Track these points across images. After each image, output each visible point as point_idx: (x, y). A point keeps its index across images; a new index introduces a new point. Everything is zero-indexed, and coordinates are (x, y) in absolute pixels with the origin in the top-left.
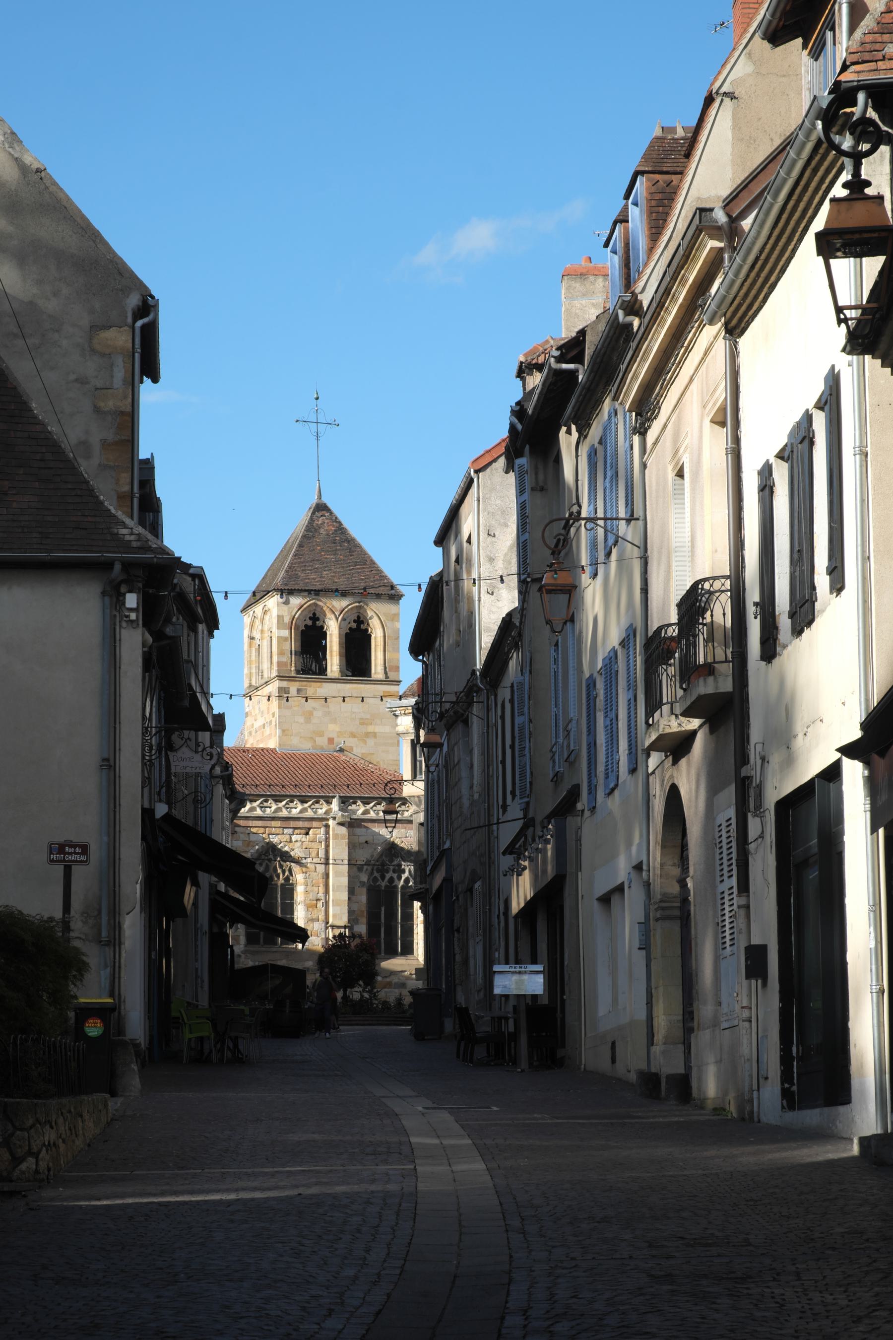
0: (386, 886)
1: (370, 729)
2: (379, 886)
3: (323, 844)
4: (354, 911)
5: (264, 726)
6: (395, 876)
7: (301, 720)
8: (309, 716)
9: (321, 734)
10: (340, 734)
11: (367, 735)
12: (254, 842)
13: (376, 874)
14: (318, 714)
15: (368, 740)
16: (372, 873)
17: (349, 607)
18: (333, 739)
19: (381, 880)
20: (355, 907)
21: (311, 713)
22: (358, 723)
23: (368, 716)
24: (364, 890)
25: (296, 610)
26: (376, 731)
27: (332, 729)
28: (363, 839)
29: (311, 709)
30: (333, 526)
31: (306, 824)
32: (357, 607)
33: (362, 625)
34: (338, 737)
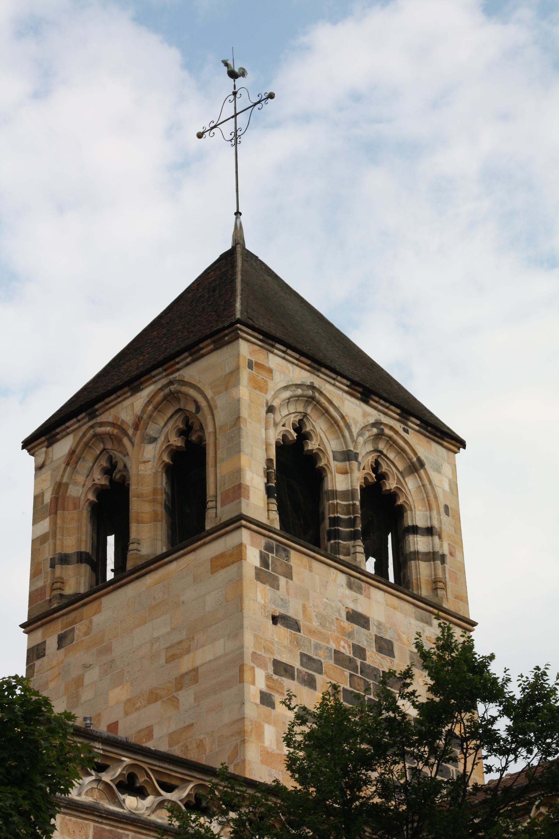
21: (79, 682)
25: (63, 466)
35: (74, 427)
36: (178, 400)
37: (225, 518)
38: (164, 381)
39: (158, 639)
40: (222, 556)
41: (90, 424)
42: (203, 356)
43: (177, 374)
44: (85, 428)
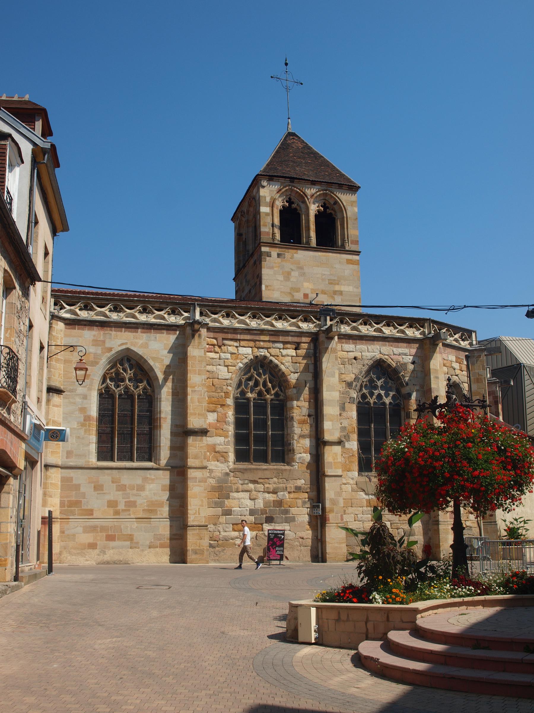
0: (375, 403)
1: (337, 288)
2: (368, 403)
3: (313, 358)
4: (345, 427)
5: (250, 291)
6: (383, 393)
7: (281, 278)
8: (287, 276)
9: (298, 290)
10: (312, 290)
11: (335, 292)
12: (243, 355)
13: (364, 391)
14: (295, 274)
15: (336, 296)
16: (361, 390)
17: (318, 193)
18: (308, 294)
19: (369, 397)
20: (345, 423)
21: (289, 274)
22: (327, 283)
23: (336, 279)
24: (354, 407)
26: (342, 289)
27: (307, 287)
28: (352, 355)
29: (290, 270)
30: (302, 144)
31: (296, 339)
32: (323, 194)
33: (328, 210)
34: (312, 293)
35: (283, 181)
36: (327, 196)
37: (352, 249)
38: (326, 188)
39: (324, 275)
40: (351, 260)
41: (290, 184)
42: (342, 189)
43: (331, 189)
44: (287, 184)
